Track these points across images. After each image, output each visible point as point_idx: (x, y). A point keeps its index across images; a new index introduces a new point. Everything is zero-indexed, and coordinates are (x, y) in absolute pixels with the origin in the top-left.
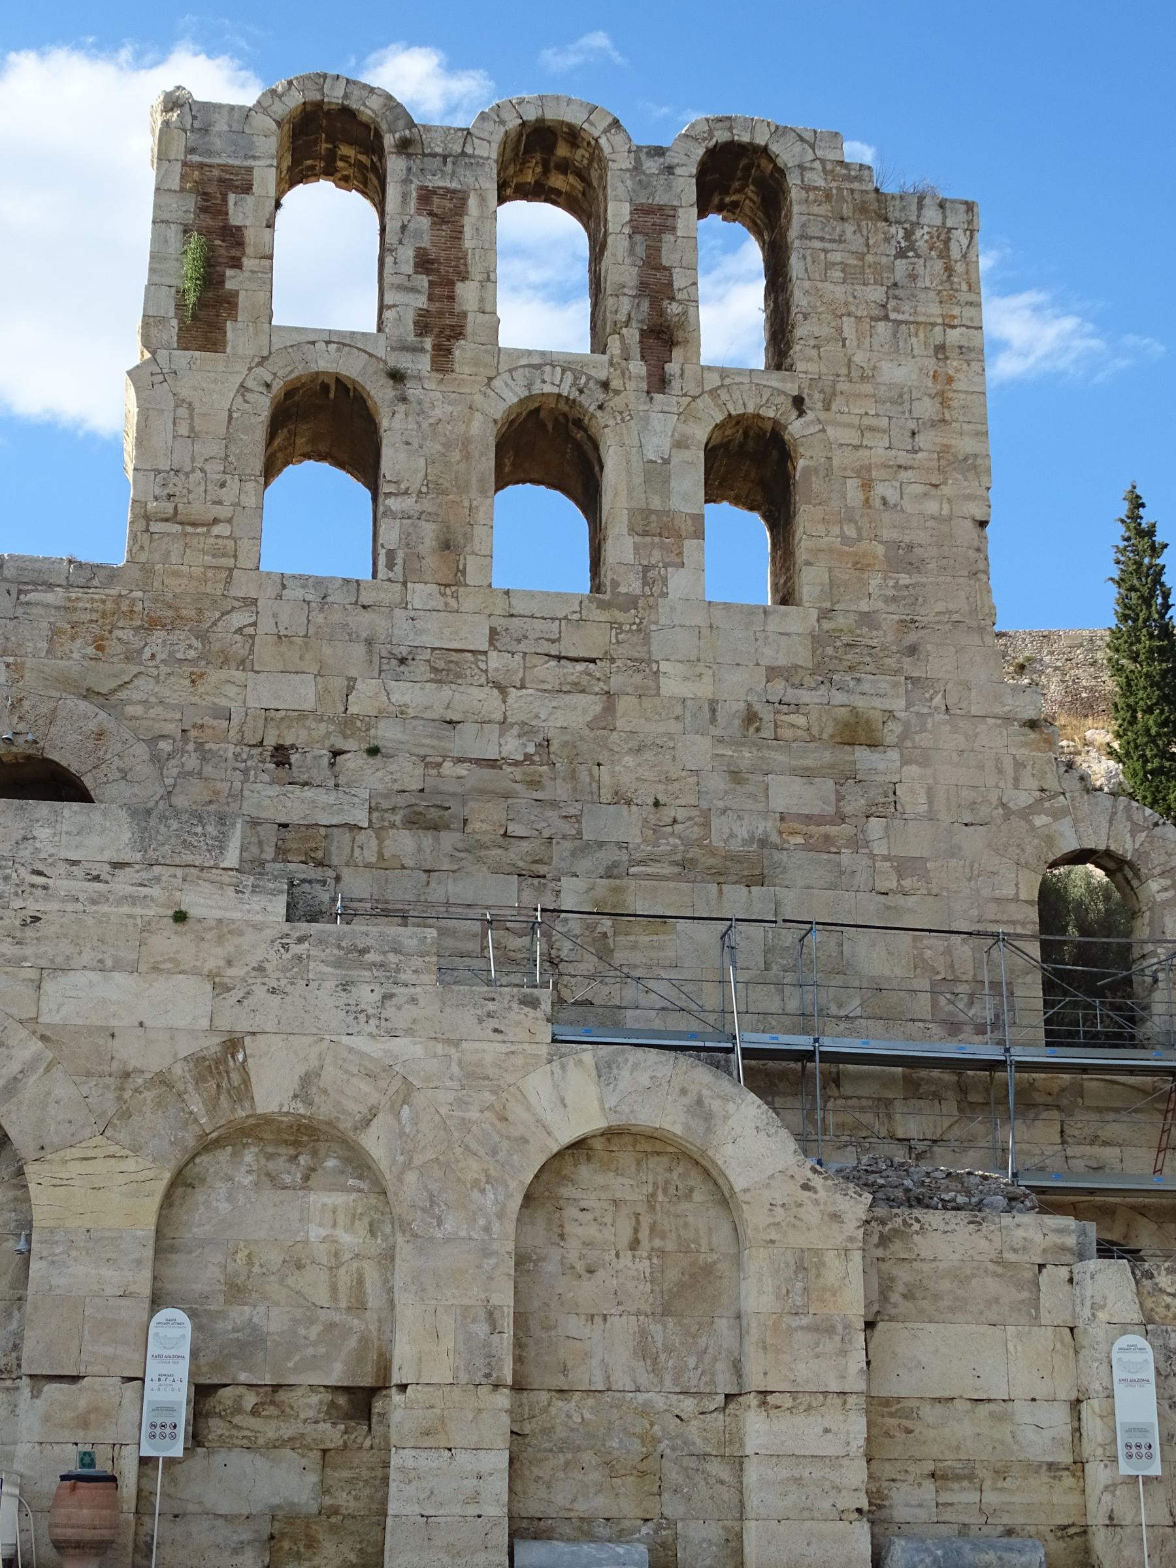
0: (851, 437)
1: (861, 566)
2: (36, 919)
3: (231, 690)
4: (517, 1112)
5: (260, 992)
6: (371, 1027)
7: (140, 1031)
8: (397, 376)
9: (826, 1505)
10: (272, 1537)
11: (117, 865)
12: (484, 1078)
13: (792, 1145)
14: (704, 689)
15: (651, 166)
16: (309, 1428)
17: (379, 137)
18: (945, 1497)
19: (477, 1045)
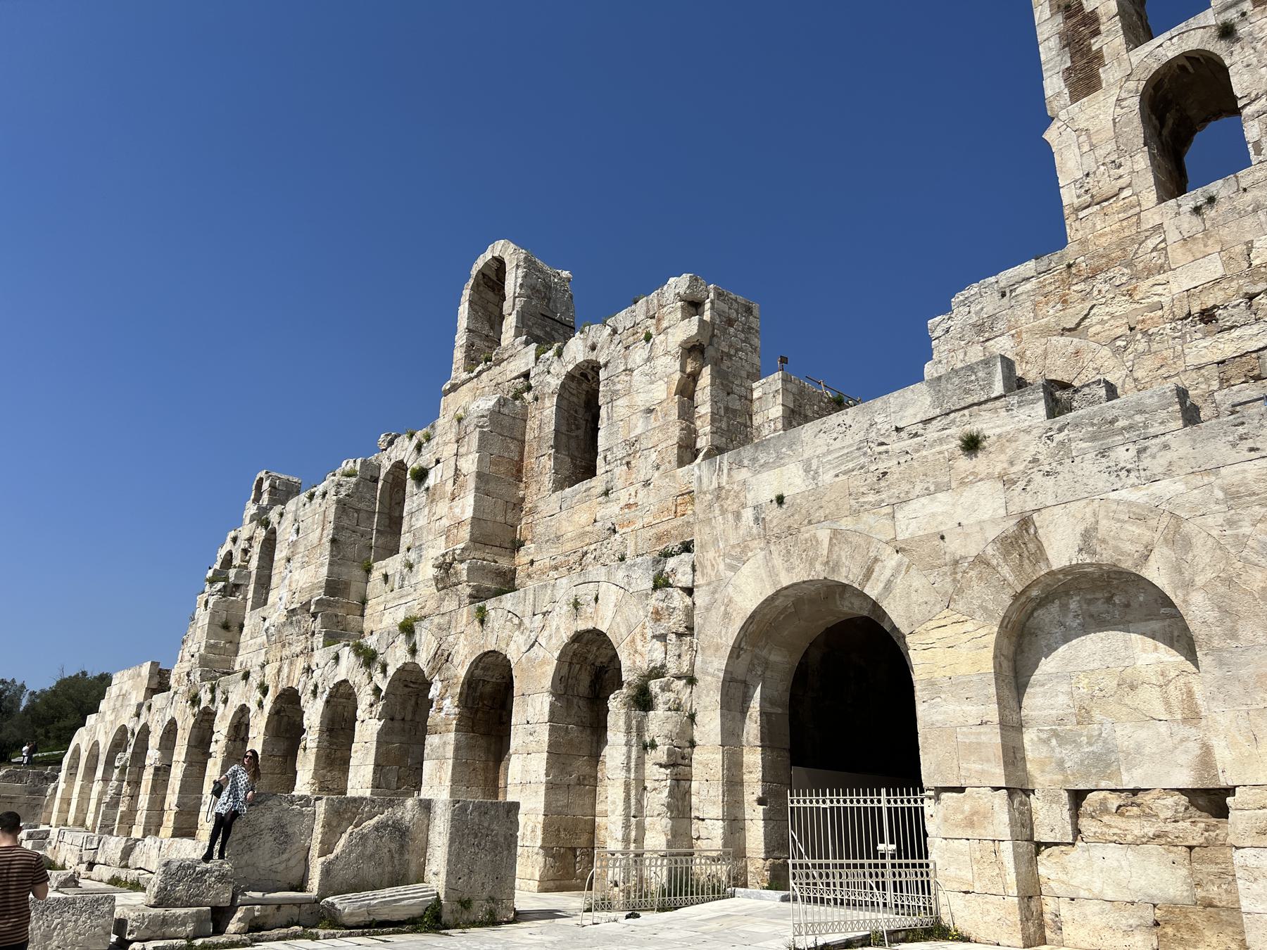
2: (885, 474)
3: (1159, 289)
5: (1038, 478)
6: (1133, 478)
7: (959, 530)
10: (1157, 924)
12: (1250, 495)
16: (1170, 827)
19: (1237, 467)
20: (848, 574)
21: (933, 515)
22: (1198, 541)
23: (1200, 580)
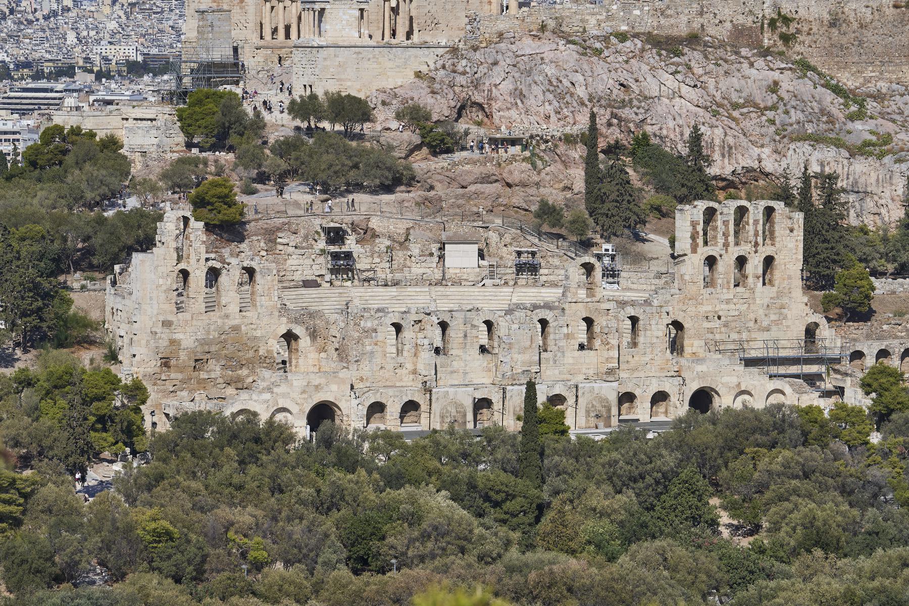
8: (721, 256)
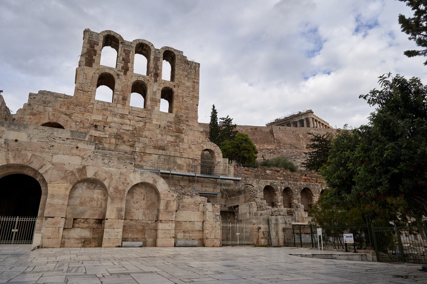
0: (181, 92)
1: (181, 109)
3: (89, 116)
4: (128, 179)
5: (89, 160)
6: (107, 166)
9: (168, 236)
11: (67, 139)
13: (168, 186)
14: (159, 123)
15: (157, 52)
17: (118, 41)
18: (185, 235)
20: (35, 165)
21: (63, 159)
22: (114, 179)
23: (112, 186)
